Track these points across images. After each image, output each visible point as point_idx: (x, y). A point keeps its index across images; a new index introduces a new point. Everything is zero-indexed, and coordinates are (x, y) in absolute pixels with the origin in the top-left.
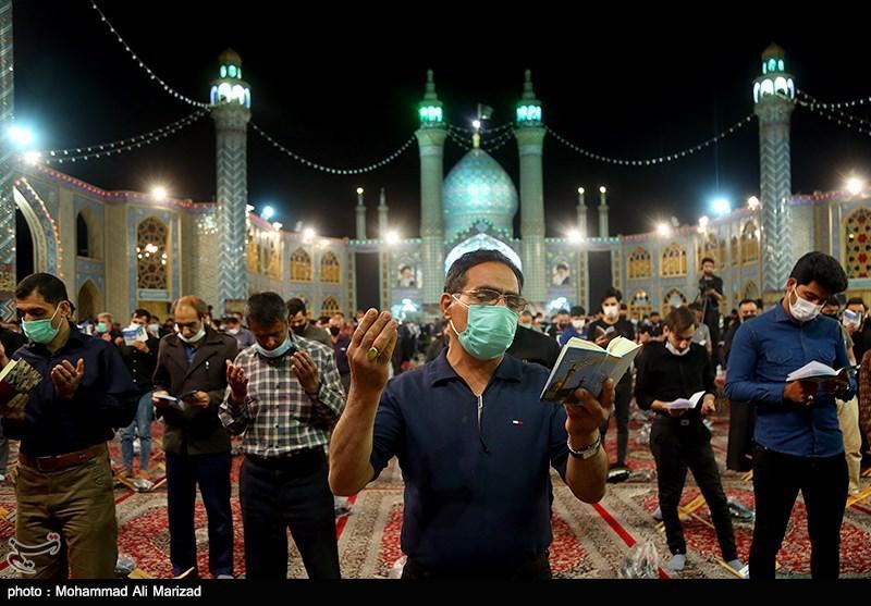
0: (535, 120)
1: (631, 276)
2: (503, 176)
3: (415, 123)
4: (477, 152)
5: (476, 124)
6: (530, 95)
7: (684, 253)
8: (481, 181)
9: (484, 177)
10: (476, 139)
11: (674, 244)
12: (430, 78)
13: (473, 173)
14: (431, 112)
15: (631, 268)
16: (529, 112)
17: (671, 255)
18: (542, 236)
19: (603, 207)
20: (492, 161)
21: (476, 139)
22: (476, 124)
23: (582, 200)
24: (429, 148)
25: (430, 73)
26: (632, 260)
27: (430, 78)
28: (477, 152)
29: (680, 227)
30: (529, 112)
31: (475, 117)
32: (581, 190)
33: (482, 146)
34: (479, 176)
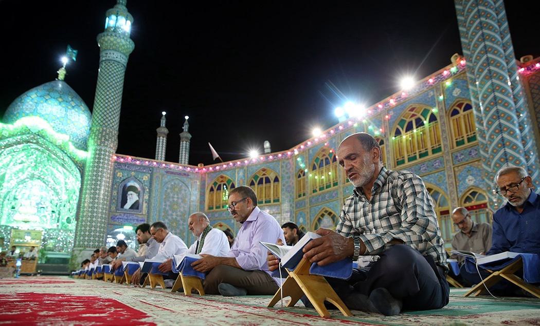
0: (125, 32)
1: (210, 208)
2: (83, 107)
7: (276, 180)
8: (57, 103)
9: (60, 100)
10: (62, 73)
11: (264, 170)
13: (48, 95)
17: (261, 182)
18: (114, 152)
20: (73, 91)
21: (62, 73)
22: (65, 60)
23: (163, 122)
26: (212, 190)
29: (272, 152)
32: (164, 113)
33: (67, 79)
34: (56, 99)
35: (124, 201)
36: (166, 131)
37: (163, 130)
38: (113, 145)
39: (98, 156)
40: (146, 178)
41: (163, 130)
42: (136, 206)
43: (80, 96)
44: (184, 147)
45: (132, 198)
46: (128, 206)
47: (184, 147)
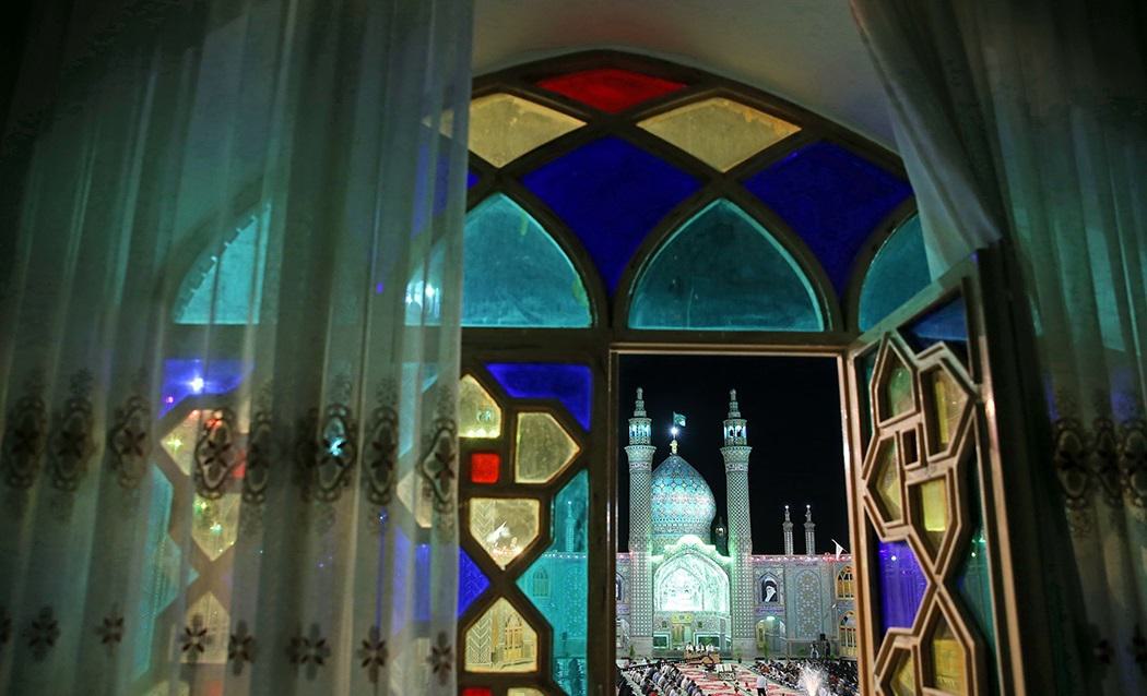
3: (625, 439)
4: (674, 460)
5: (674, 431)
6: (738, 414)
10: (674, 445)
12: (640, 396)
14: (640, 428)
15: (840, 589)
16: (736, 428)
19: (809, 525)
21: (674, 445)
22: (674, 431)
24: (639, 455)
25: (640, 391)
26: (840, 578)
27: (640, 396)
28: (674, 460)
30: (736, 428)
31: (670, 421)
33: (680, 452)
35: (765, 596)
36: (791, 525)
37: (788, 525)
38: (749, 547)
39: (740, 560)
40: (780, 572)
41: (788, 525)
42: (774, 598)
43: (705, 479)
44: (810, 538)
45: (771, 592)
46: (767, 600)
47: (810, 538)
